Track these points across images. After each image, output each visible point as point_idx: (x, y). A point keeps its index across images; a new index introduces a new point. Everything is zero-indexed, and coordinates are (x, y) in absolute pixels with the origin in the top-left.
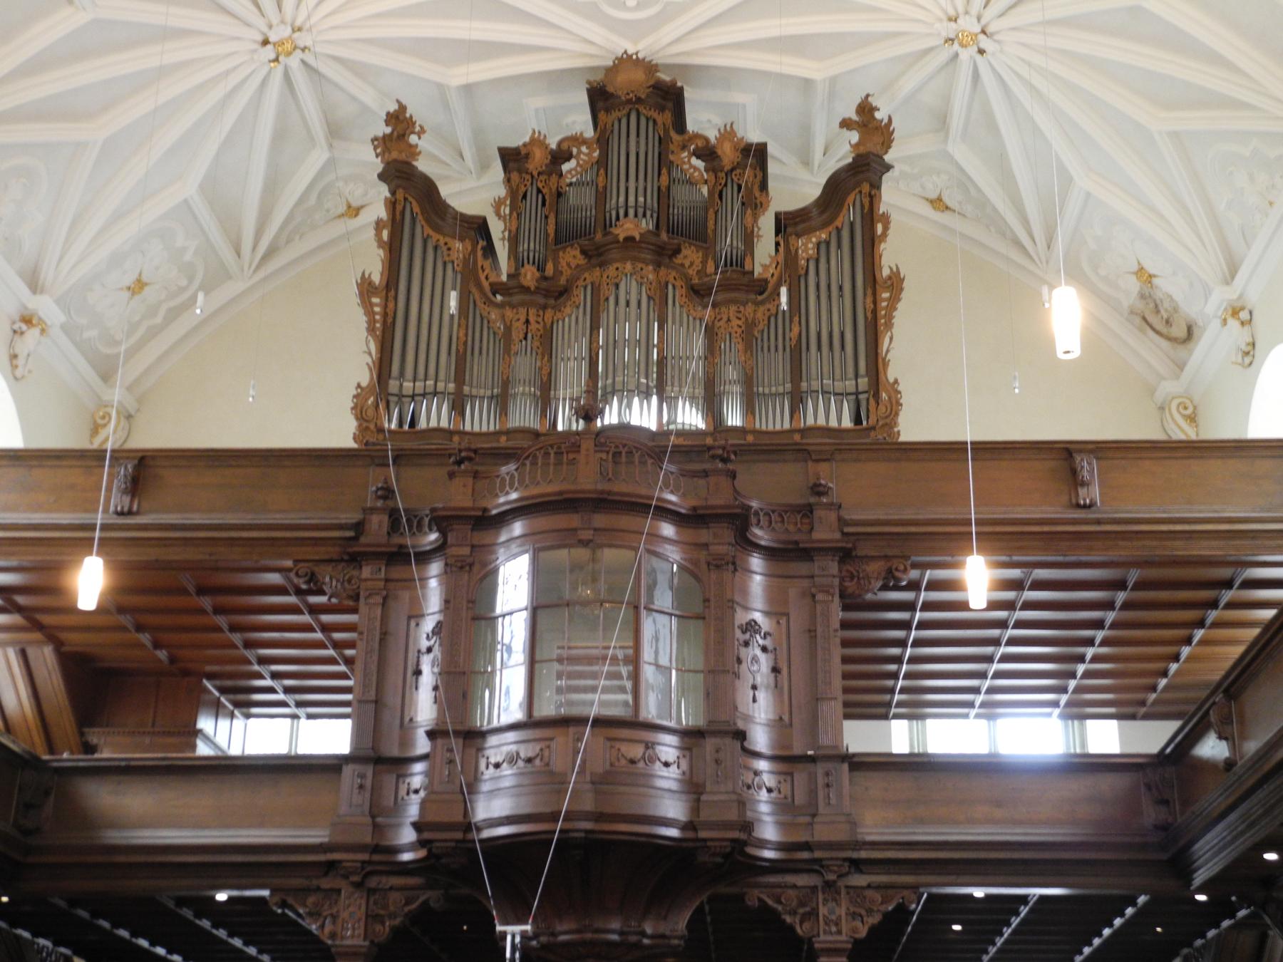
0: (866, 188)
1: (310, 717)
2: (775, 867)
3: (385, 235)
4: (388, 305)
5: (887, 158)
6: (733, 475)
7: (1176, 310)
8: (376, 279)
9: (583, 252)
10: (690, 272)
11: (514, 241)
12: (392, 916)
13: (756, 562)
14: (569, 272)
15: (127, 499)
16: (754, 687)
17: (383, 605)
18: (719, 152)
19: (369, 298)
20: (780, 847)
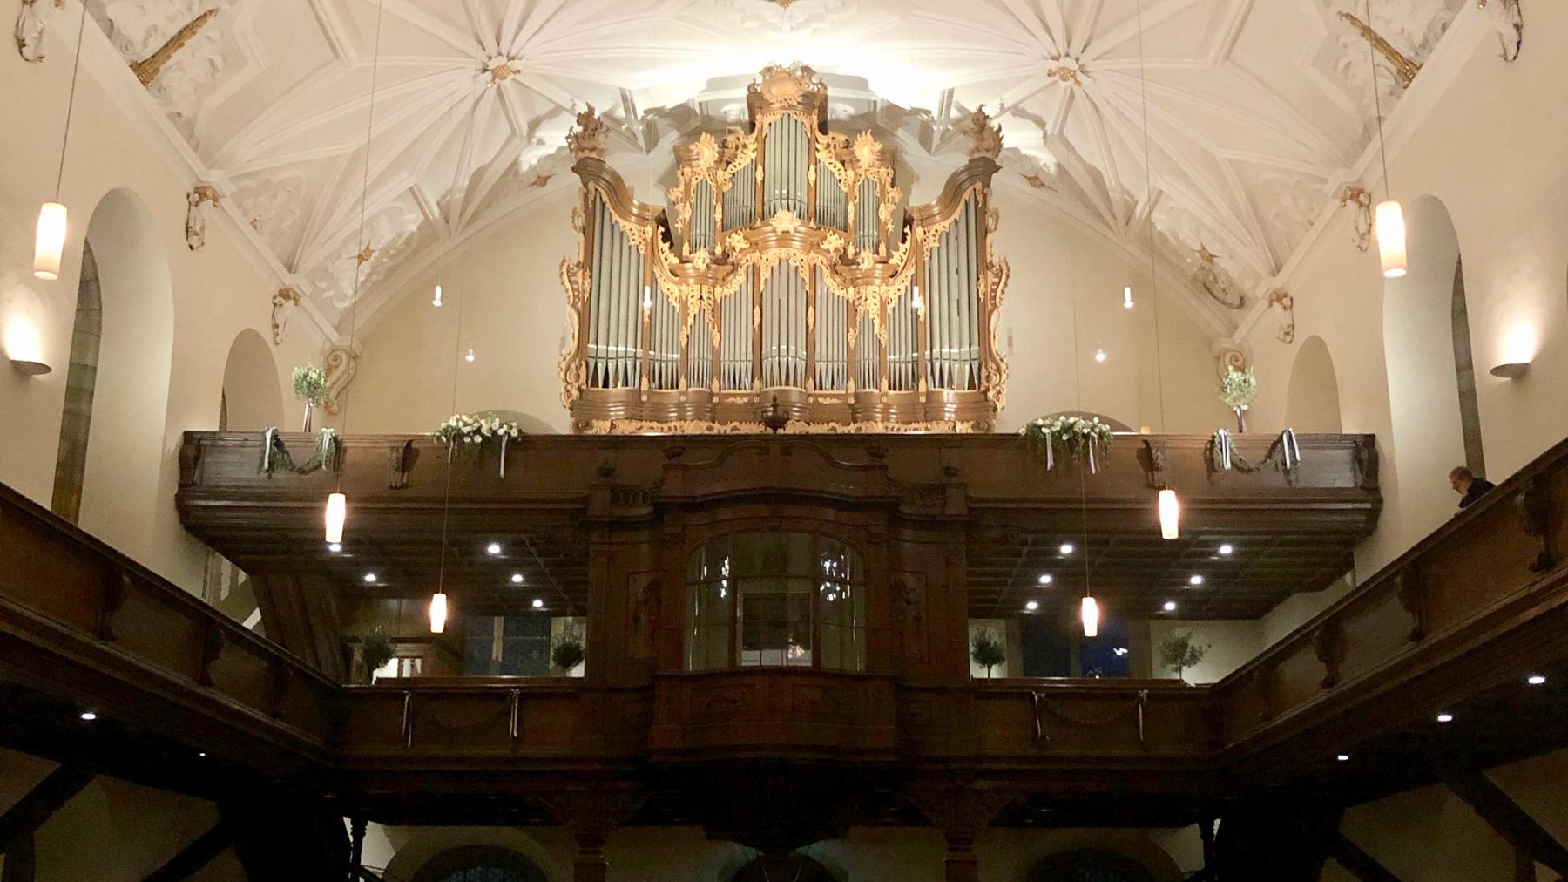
6: (885, 468)
7: (1231, 282)
15: (398, 475)
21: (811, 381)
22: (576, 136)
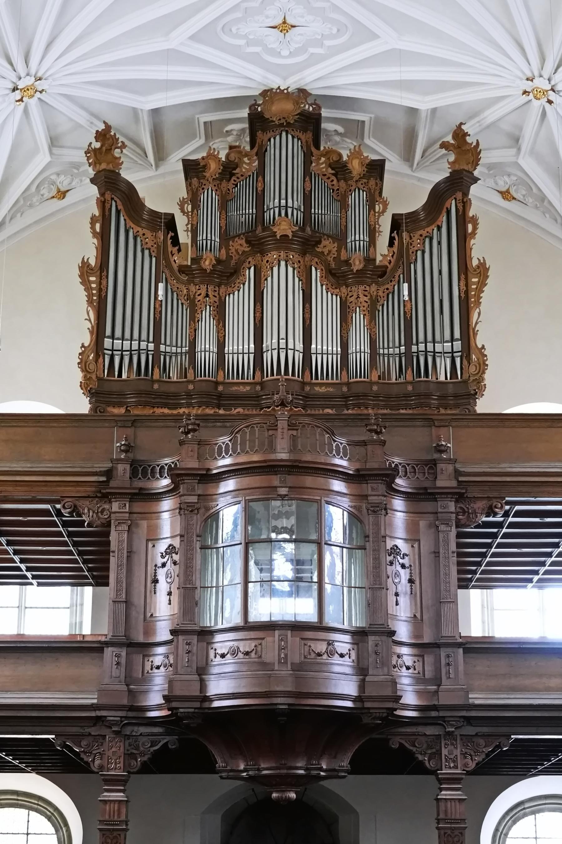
0: (459, 195)
1: (39, 584)
2: (412, 721)
3: (98, 227)
4: (96, 276)
5: (476, 173)
6: (384, 443)
8: (92, 262)
9: (247, 242)
10: (329, 259)
11: (194, 232)
12: (142, 754)
13: (398, 504)
14: (237, 257)
16: (397, 595)
17: (128, 531)
18: (350, 166)
19: (88, 277)
20: (417, 708)
21: (307, 373)
22: (95, 150)
